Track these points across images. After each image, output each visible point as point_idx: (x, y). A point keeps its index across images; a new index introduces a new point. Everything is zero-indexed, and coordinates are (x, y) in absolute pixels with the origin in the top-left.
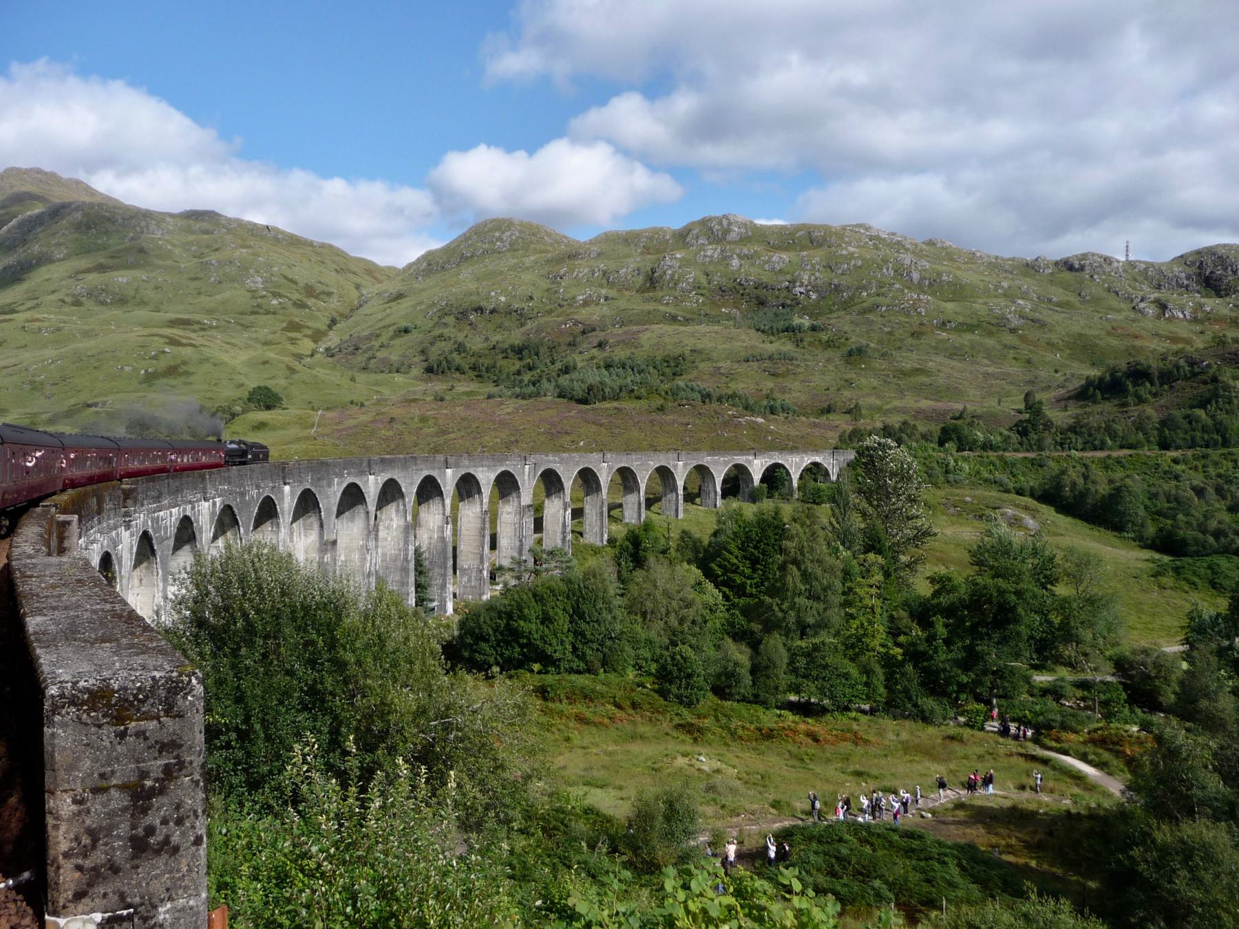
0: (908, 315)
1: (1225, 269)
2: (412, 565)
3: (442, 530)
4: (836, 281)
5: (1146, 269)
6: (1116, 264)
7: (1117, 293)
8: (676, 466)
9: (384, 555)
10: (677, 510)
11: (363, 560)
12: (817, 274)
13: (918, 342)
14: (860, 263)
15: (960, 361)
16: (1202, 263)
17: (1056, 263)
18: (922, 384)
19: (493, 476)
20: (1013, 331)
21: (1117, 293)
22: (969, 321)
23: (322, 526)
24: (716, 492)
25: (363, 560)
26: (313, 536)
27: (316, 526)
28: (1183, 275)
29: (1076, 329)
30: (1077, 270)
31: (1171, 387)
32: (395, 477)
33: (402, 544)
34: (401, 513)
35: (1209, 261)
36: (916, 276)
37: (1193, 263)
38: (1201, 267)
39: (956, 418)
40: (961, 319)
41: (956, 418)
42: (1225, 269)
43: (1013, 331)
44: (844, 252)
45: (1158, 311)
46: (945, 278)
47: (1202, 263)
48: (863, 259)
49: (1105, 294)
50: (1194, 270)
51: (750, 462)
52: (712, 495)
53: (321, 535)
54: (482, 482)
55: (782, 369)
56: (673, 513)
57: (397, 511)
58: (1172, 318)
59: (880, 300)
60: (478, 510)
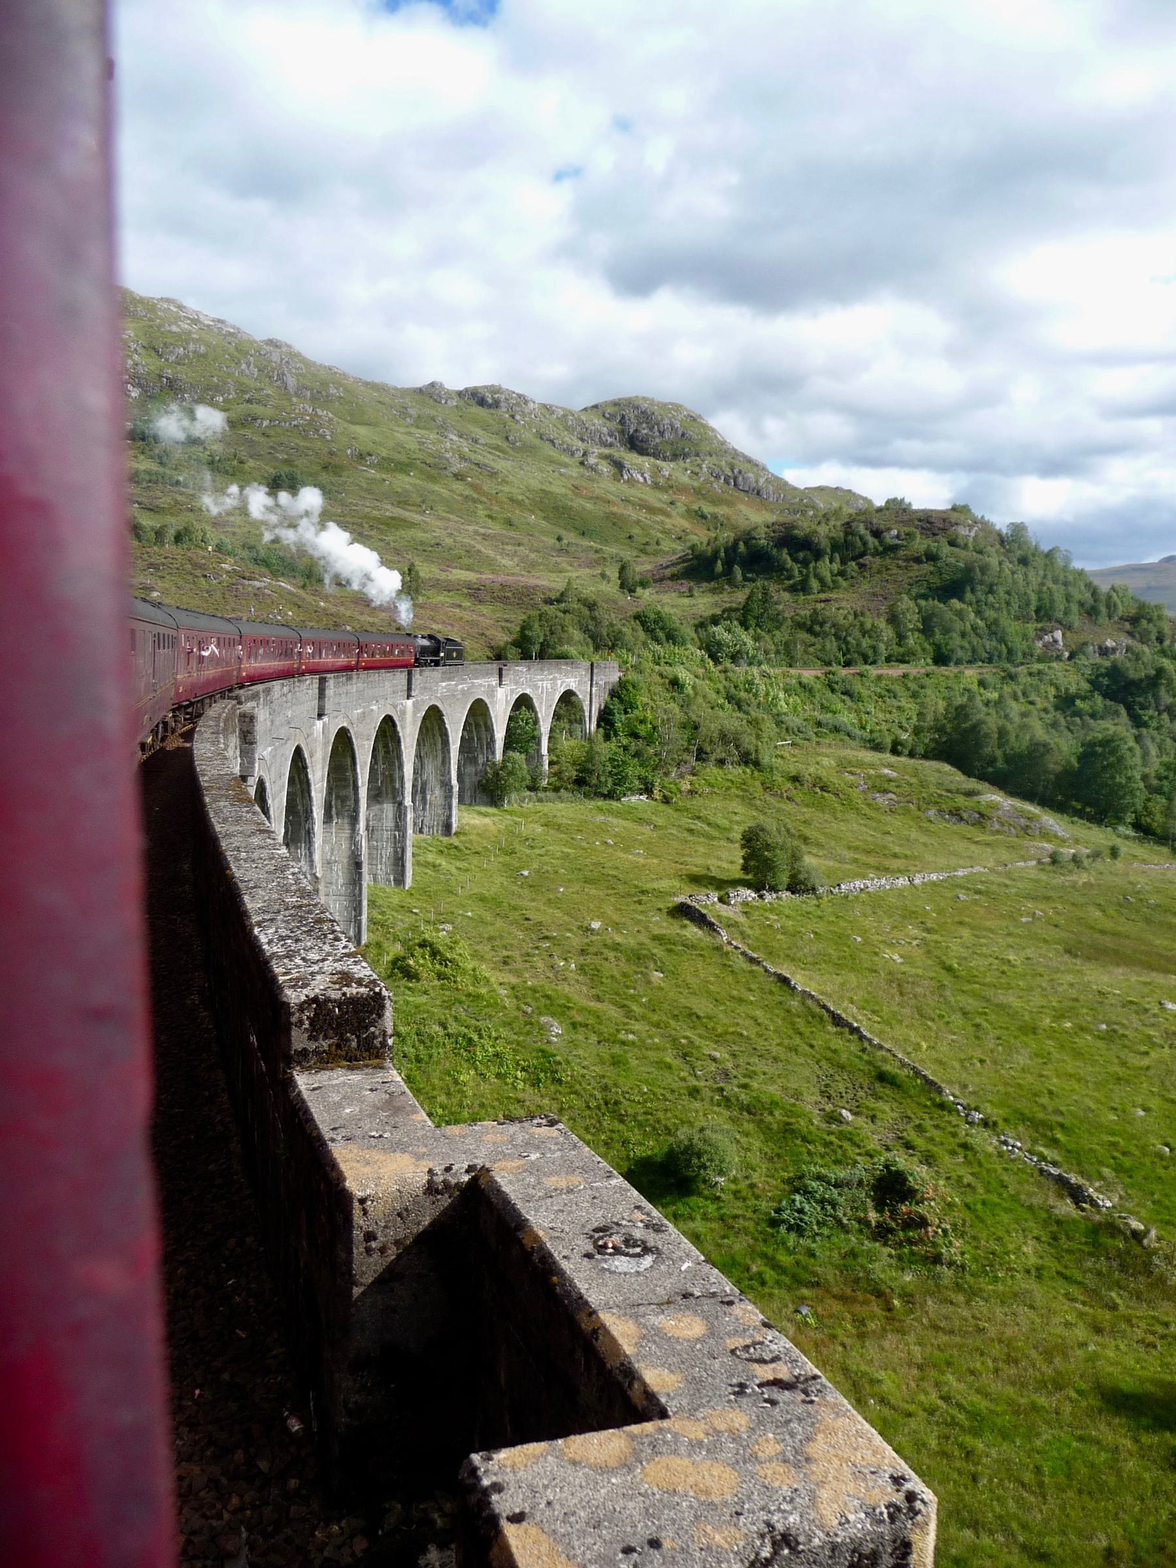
0: (306, 437)
1: (651, 429)
4: (169, 372)
5: (565, 416)
6: (531, 405)
7: (552, 442)
8: (403, 713)
10: (399, 861)
12: (136, 357)
13: (335, 479)
14: (203, 349)
15: (417, 513)
16: (623, 417)
17: (460, 394)
18: (422, 543)
20: (458, 477)
21: (552, 442)
22: (397, 456)
24: (446, 785)
28: (605, 430)
29: (535, 484)
30: (490, 406)
31: (862, 566)
35: (631, 415)
36: (291, 382)
37: (611, 418)
38: (622, 421)
39: (549, 601)
40: (384, 453)
41: (549, 601)
42: (651, 429)
43: (458, 477)
44: (174, 329)
45: (613, 470)
46: (332, 391)
47: (623, 417)
48: (208, 345)
49: (537, 442)
50: (614, 425)
51: (491, 692)
52: (435, 795)
55: (164, 501)
56: (384, 869)
58: (631, 482)
59: (257, 409)
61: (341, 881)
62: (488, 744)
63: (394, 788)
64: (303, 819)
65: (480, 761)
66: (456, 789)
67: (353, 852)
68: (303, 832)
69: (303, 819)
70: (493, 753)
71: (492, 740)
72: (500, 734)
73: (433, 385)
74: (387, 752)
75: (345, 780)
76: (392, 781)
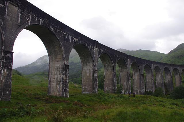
2: (164, 84)
3: (170, 79)
9: (158, 82)
11: (152, 81)
19: (182, 69)
23: (140, 71)
25: (152, 81)
26: (138, 73)
27: (139, 71)
32: (158, 66)
33: (161, 80)
34: (161, 74)
53: (140, 73)
54: (179, 70)
57: (160, 73)
60: (179, 76)
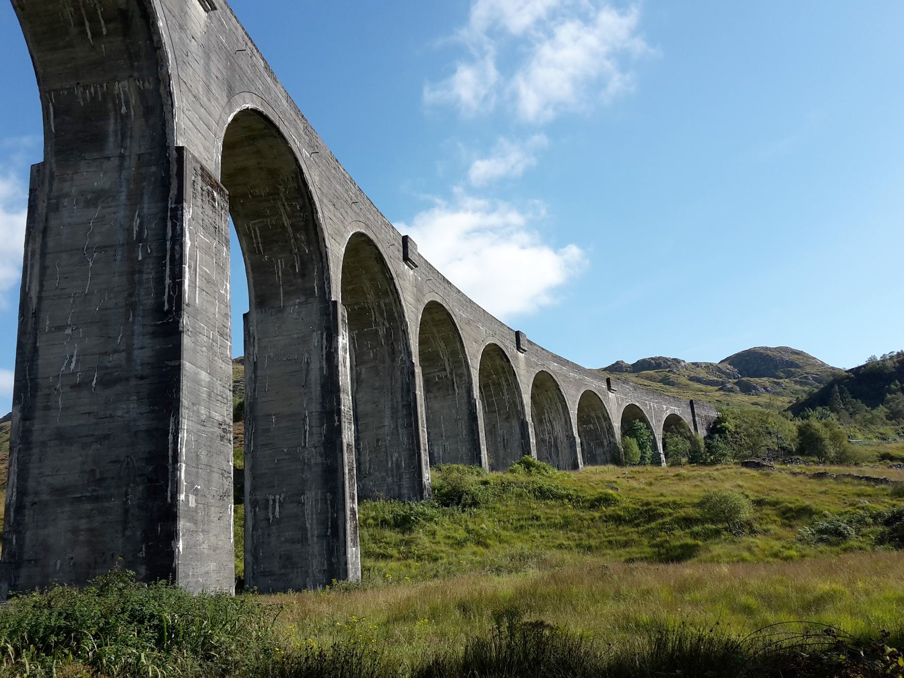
61: (465, 432)
62: (608, 430)
63: (517, 411)
64: (399, 324)
65: (606, 444)
66: (578, 440)
67: (470, 411)
68: (401, 333)
69: (399, 324)
70: (613, 436)
71: (610, 427)
72: (617, 424)
73: (617, 363)
74: (508, 385)
75: (460, 361)
76: (516, 406)
